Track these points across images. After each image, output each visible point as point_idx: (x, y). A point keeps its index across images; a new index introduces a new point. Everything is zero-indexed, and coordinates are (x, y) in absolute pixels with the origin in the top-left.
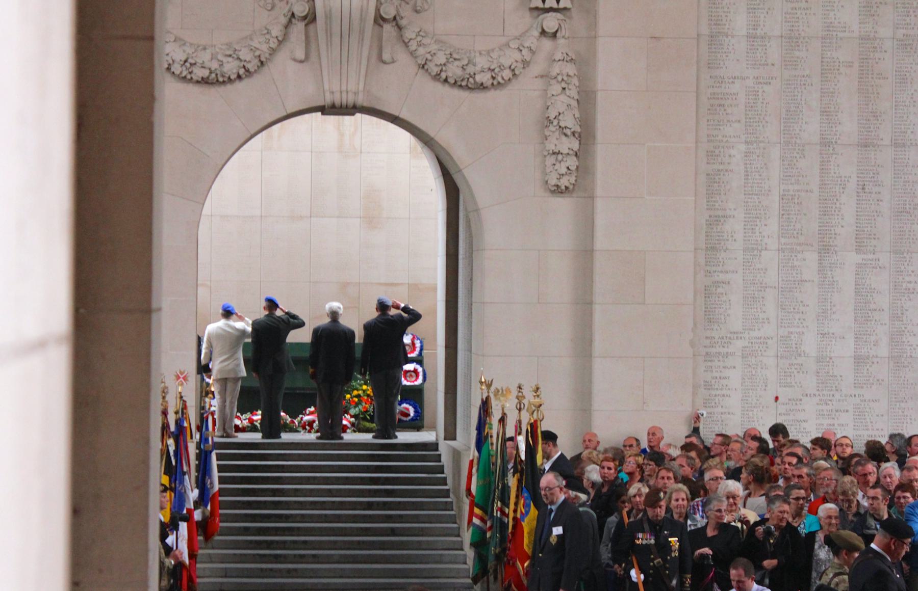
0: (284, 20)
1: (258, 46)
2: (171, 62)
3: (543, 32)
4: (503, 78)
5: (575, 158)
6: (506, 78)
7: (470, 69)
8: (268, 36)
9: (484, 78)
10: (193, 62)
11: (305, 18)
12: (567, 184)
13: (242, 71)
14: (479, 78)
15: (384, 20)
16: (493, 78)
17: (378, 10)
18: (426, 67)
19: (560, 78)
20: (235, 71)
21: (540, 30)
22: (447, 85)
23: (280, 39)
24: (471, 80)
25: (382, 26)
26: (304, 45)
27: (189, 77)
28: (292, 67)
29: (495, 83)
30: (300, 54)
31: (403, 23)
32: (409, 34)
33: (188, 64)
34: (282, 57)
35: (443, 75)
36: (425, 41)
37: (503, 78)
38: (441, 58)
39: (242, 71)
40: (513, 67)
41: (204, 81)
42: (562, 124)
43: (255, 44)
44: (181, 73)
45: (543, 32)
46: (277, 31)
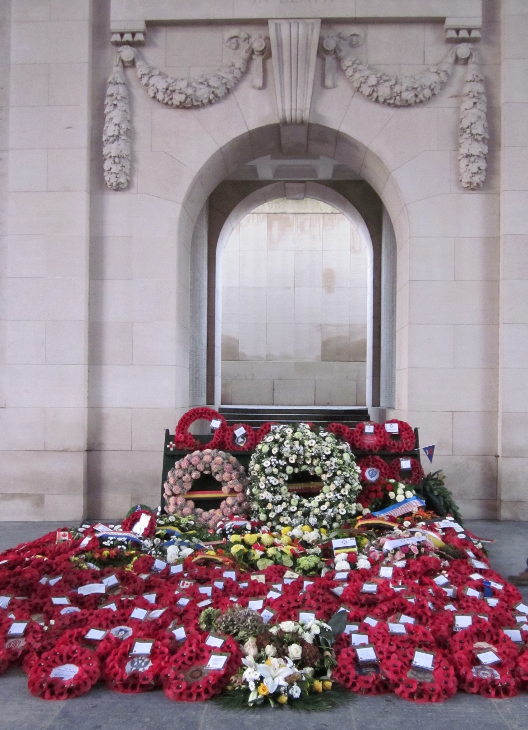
1: (224, 75)
3: (457, 60)
4: (424, 97)
5: (484, 161)
6: (427, 97)
7: (397, 89)
8: (232, 68)
9: (409, 96)
12: (478, 181)
14: (405, 95)
15: (327, 52)
18: (361, 90)
19: (471, 95)
21: (454, 58)
23: (242, 70)
24: (398, 98)
25: (324, 59)
26: (262, 74)
27: (170, 102)
28: (253, 94)
29: (418, 101)
30: (259, 82)
31: (342, 54)
33: (168, 91)
34: (245, 86)
35: (375, 95)
37: (424, 97)
38: (373, 81)
39: (212, 96)
40: (432, 87)
41: (182, 106)
42: (474, 132)
43: (222, 74)
44: (164, 99)
46: (239, 64)
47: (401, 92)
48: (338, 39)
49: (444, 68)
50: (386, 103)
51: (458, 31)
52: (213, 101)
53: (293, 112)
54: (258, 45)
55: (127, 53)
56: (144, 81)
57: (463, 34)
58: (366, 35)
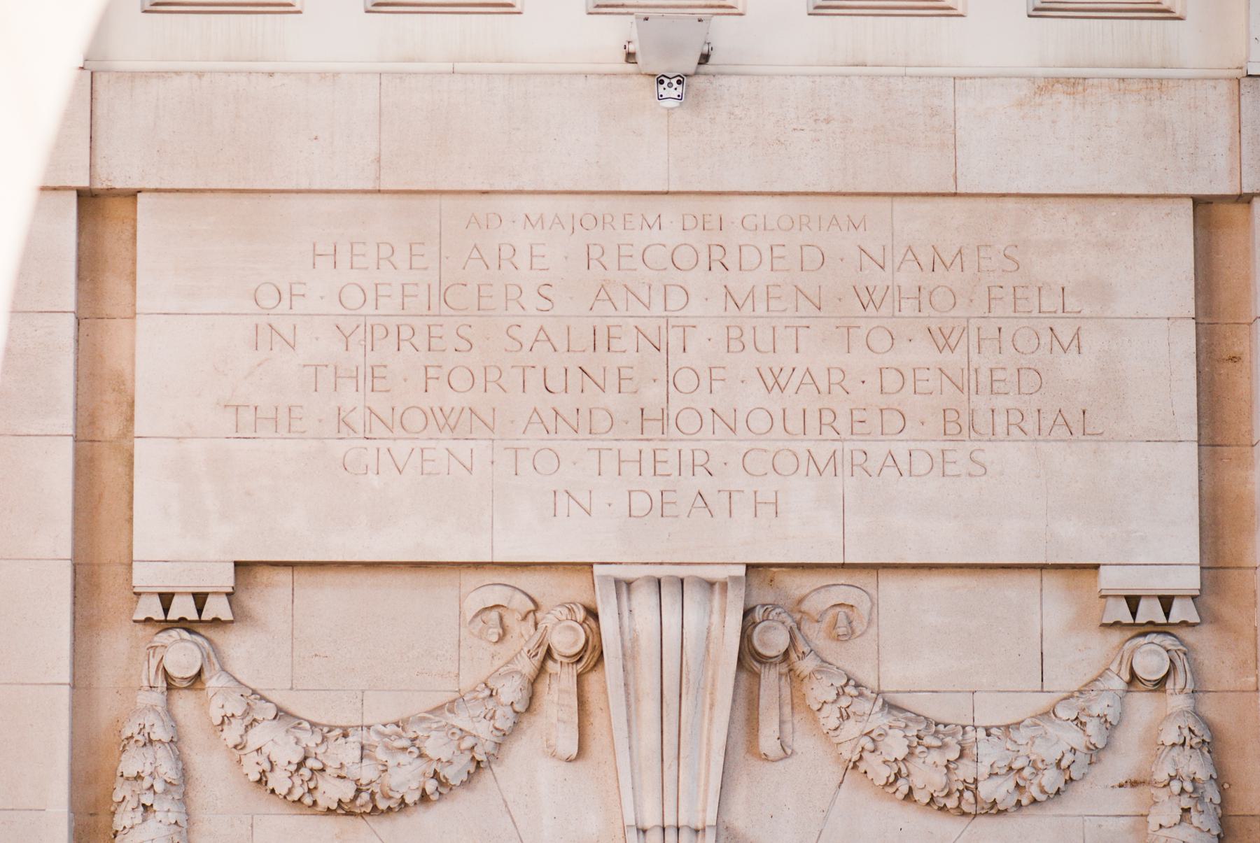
1: (467, 726)
4: (1043, 791)
7: (965, 771)
8: (491, 704)
9: (997, 790)
10: (318, 765)
11: (578, 657)
13: (431, 786)
14: (987, 790)
15: (762, 659)
18: (862, 766)
20: (414, 785)
21: (1127, 677)
22: (910, 807)
23: (518, 708)
24: (968, 795)
25: (757, 675)
28: (548, 774)
29: (1025, 802)
33: (305, 772)
34: (522, 750)
35: (903, 786)
37: (1043, 791)
38: (896, 746)
39: (431, 786)
43: (461, 720)
44: (290, 791)
46: (511, 691)
51: (1133, 602)
52: (435, 797)
55: (182, 654)
56: (232, 734)
58: (874, 604)
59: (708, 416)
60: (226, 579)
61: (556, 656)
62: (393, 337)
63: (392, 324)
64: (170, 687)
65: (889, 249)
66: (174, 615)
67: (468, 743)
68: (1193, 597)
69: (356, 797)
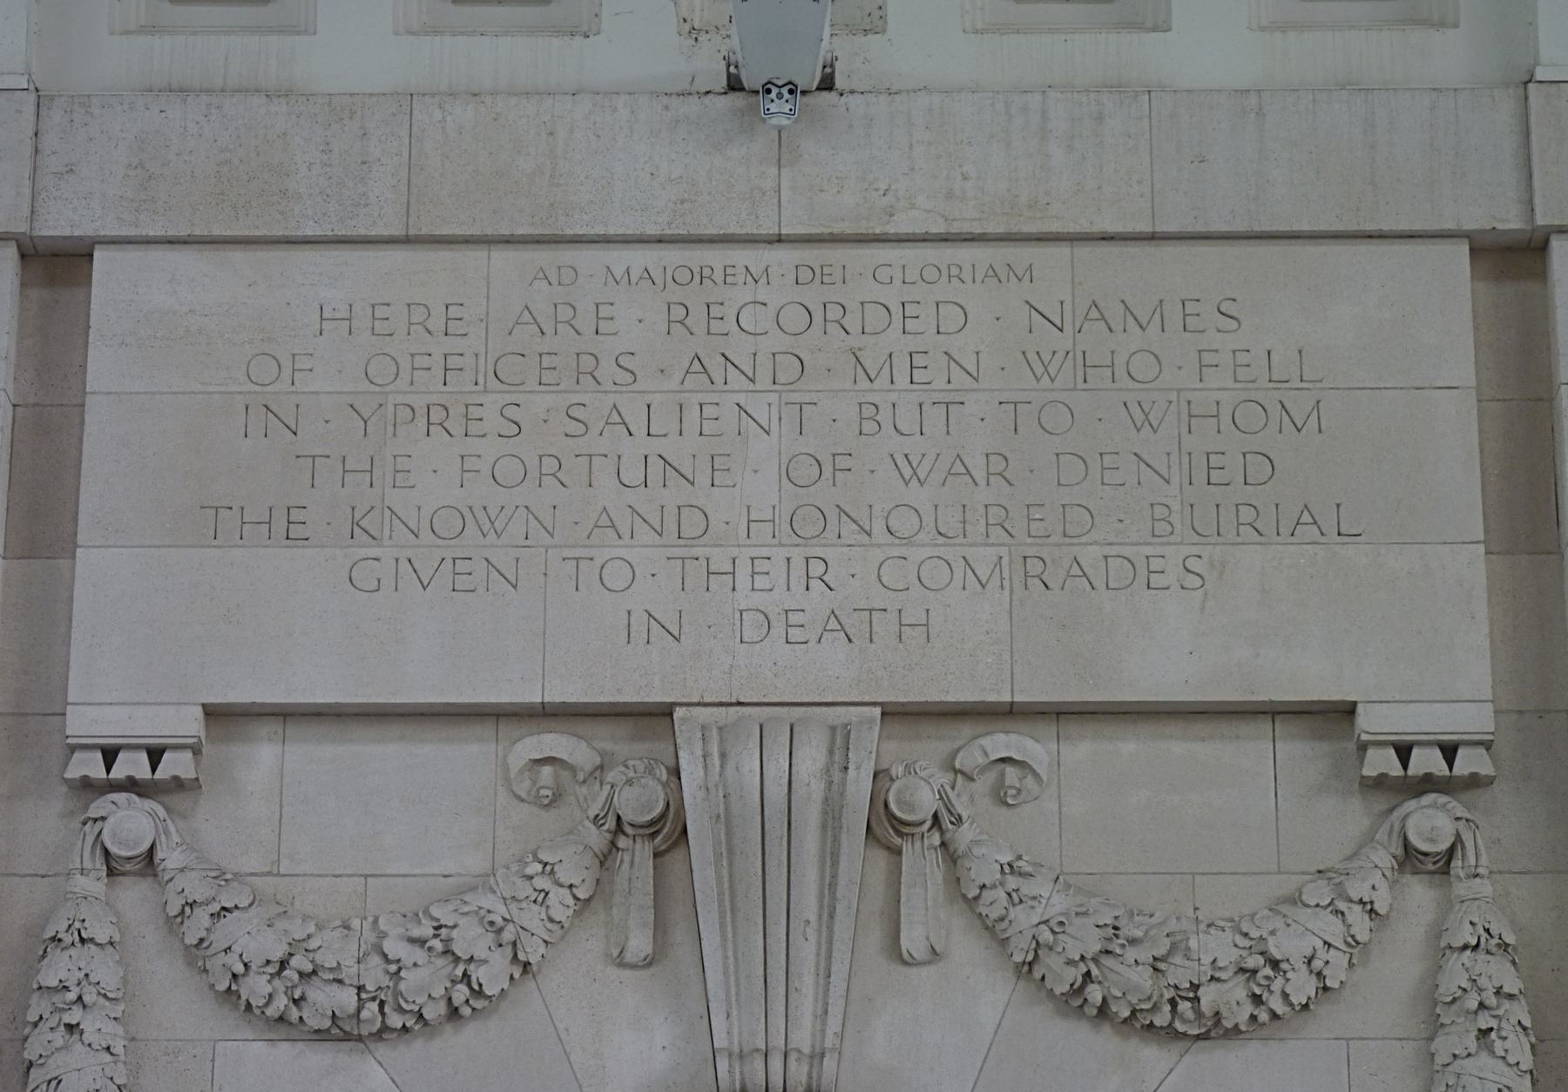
0: (597, 838)
2: (240, 968)
6: (1298, 999)
7: (1179, 973)
9: (1230, 999)
13: (461, 993)
16: (1257, 999)
17: (879, 806)
19: (1473, 1004)
20: (438, 992)
22: (1106, 1028)
24: (1184, 1006)
25: (899, 853)
27: (294, 1014)
29: (1264, 1016)
30: (640, 944)
31: (964, 837)
32: (982, 870)
35: (1095, 994)
36: (1028, 888)
39: (461, 993)
41: (339, 1032)
45: (1409, 857)
47: (1195, 987)
48: (945, 779)
49: (1357, 890)
50: (1138, 1025)
52: (466, 1011)
53: (776, 1064)
54: (640, 800)
55: (130, 823)
57: (1426, 761)
59: (832, 514)
60: (191, 724)
61: (629, 830)
62: (421, 422)
63: (420, 402)
64: (111, 872)
65: (1068, 307)
66: (119, 772)
67: (508, 936)
68: (1488, 745)
69: (359, 1011)
